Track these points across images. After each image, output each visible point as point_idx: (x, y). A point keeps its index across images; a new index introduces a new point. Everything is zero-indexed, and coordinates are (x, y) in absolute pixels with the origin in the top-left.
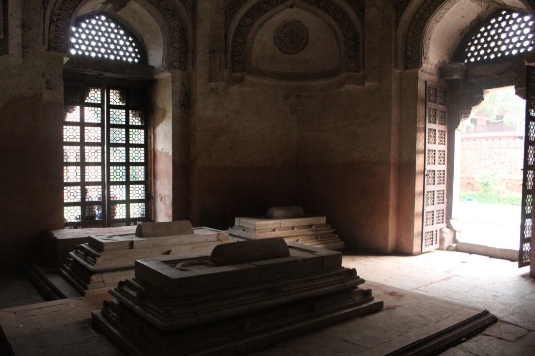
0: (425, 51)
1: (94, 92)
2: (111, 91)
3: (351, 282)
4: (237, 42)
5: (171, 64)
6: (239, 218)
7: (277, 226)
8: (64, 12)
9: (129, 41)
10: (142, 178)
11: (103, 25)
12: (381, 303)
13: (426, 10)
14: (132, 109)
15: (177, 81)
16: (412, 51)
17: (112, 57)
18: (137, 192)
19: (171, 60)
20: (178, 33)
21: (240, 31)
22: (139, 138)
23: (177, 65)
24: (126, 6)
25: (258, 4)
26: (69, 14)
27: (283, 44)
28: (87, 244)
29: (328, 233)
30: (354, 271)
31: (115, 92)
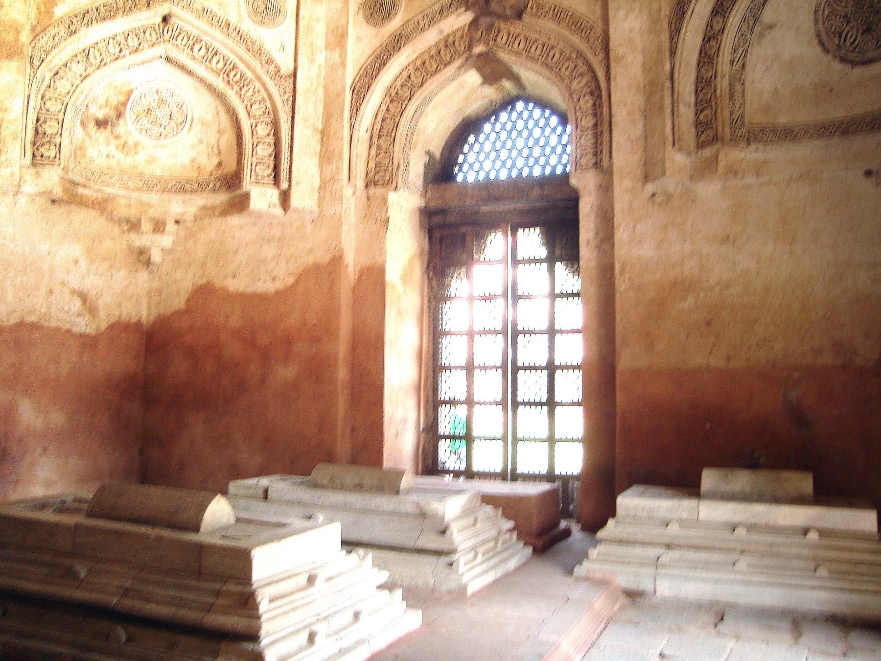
14: (561, 259)
27: (848, 43)
29: (849, 562)
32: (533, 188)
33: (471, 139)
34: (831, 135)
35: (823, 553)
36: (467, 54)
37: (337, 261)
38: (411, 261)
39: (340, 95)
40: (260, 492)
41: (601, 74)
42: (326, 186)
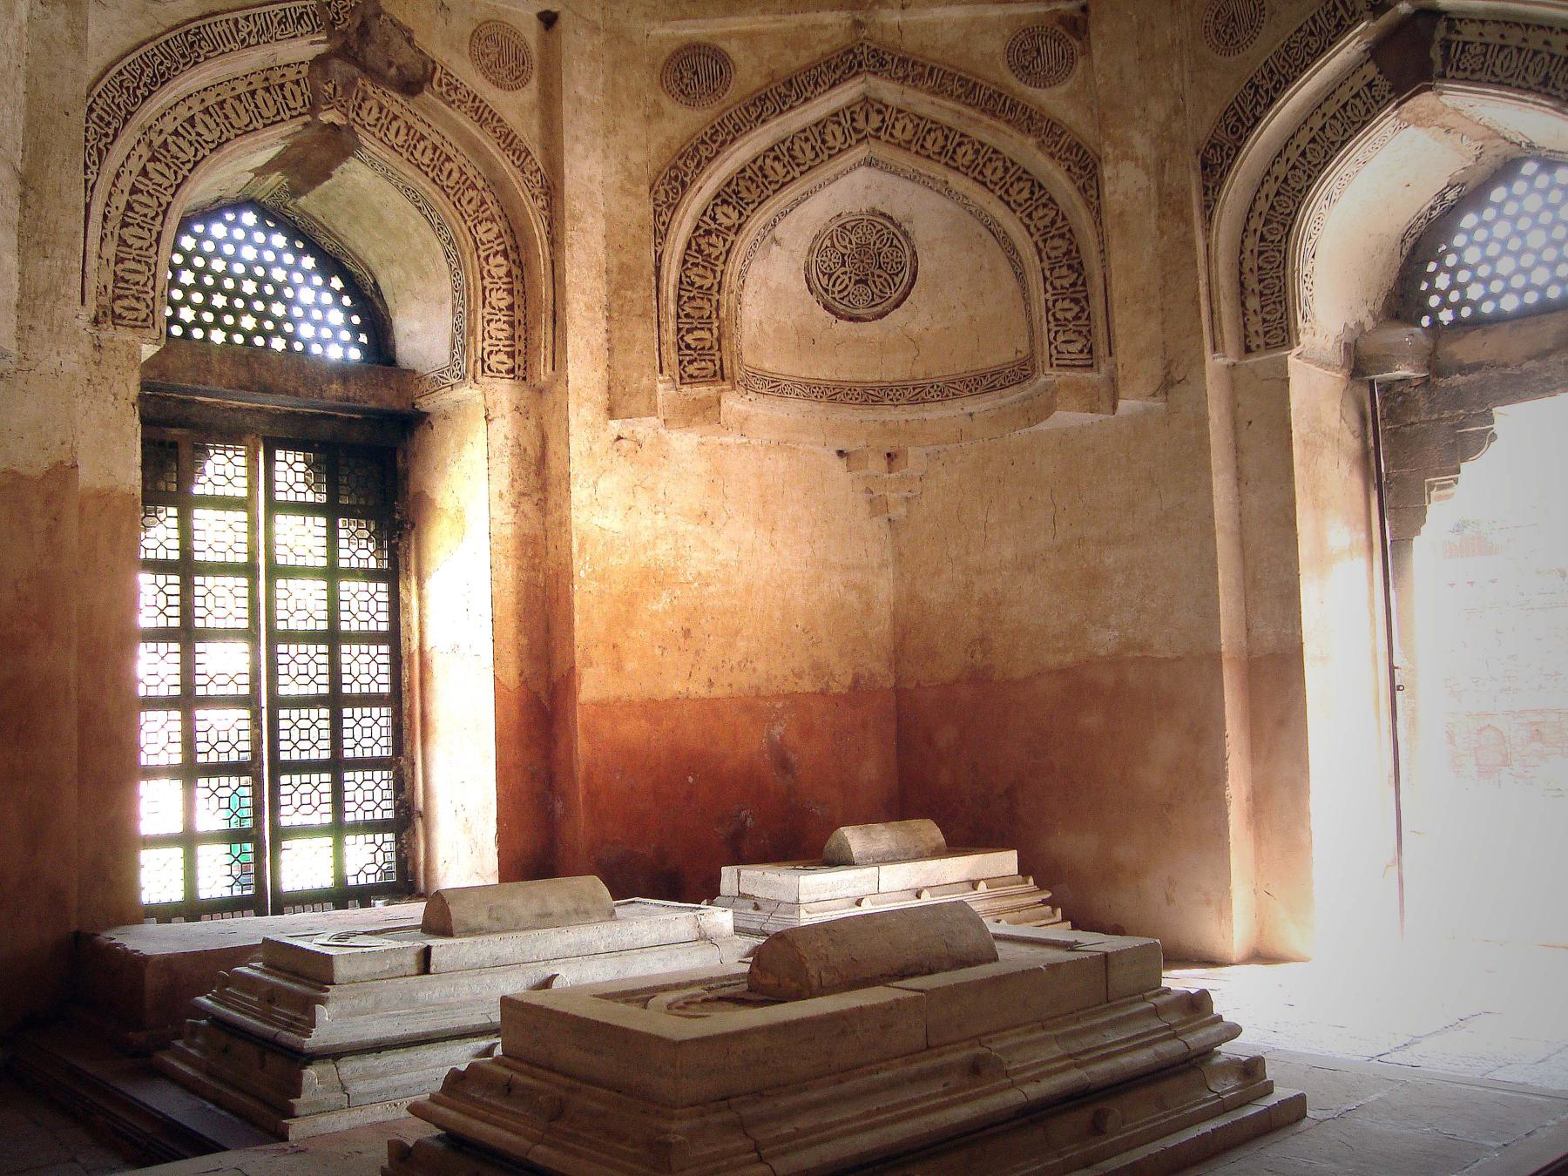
0: (1304, 293)
1: (223, 459)
2: (280, 455)
3: (1201, 1034)
4: (692, 284)
5: (483, 361)
6: (735, 868)
7: (869, 887)
8: (144, 199)
9: (333, 291)
10: (382, 749)
11: (249, 239)
12: (1300, 1101)
13: (1294, 167)
14: (349, 512)
15: (503, 416)
16: (1262, 294)
17: (278, 344)
18: (369, 795)
20: (500, 260)
21: (700, 251)
22: (373, 611)
24: (329, 176)
25: (754, 162)
26: (160, 205)
28: (259, 965)
30: (1204, 994)
31: (290, 458)
32: (330, 382)
34: (817, 399)
35: (998, 904)
36: (308, 118)
40: (410, 961)
41: (539, 230)
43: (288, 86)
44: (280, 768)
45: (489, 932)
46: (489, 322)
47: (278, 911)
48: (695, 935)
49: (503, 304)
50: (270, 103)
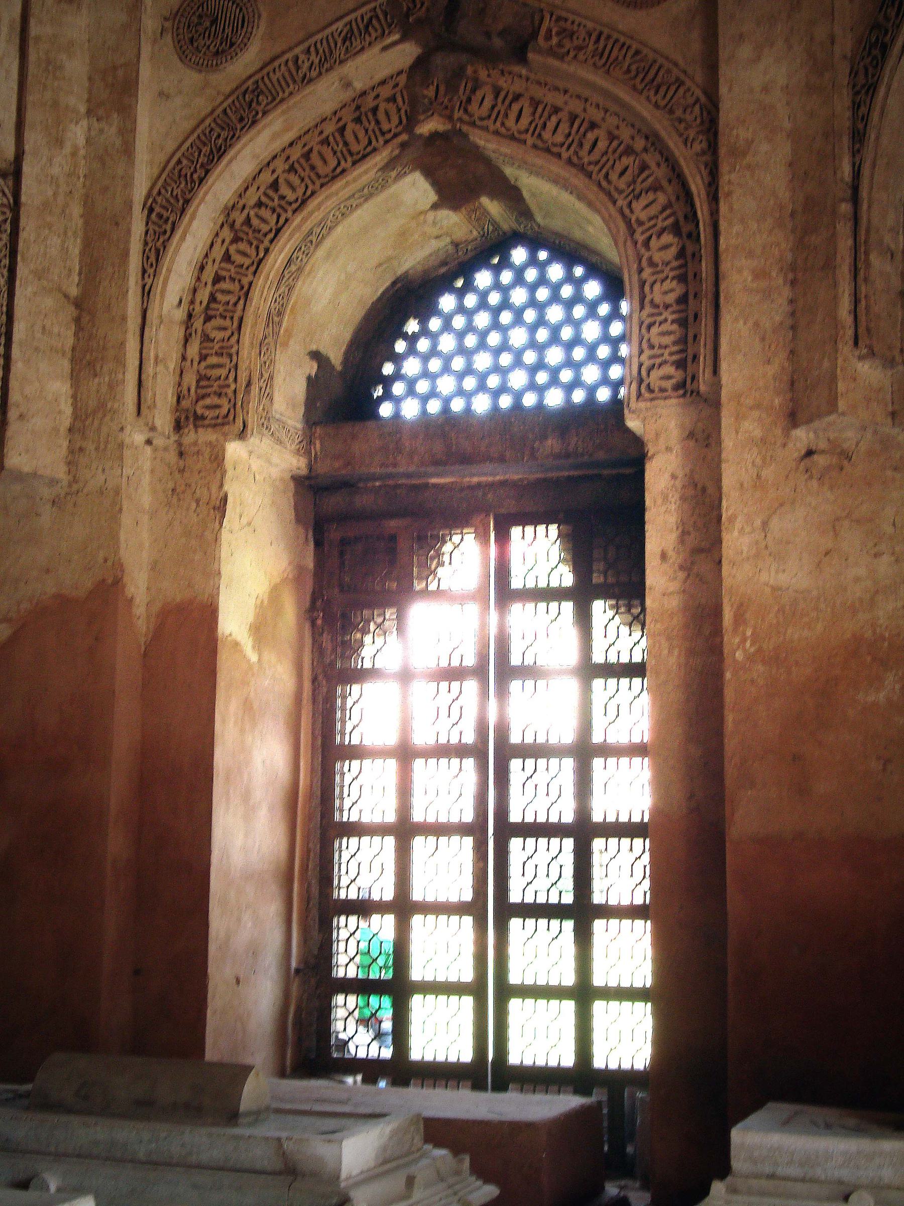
14: (604, 592)
15: (669, 449)
19: (641, 365)
20: (667, 238)
23: (669, 377)
26: (242, 288)
32: (544, 437)
33: (412, 326)
36: (404, 137)
37: (109, 590)
38: (275, 592)
39: (119, 220)
41: (697, 186)
42: (88, 425)
43: (383, 106)
44: (507, 911)
45: (69, 1111)
46: (649, 327)
47: (500, 1085)
48: (279, 1166)
49: (671, 298)
50: (361, 134)
